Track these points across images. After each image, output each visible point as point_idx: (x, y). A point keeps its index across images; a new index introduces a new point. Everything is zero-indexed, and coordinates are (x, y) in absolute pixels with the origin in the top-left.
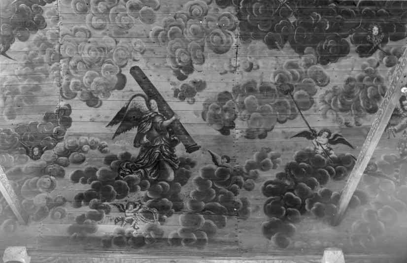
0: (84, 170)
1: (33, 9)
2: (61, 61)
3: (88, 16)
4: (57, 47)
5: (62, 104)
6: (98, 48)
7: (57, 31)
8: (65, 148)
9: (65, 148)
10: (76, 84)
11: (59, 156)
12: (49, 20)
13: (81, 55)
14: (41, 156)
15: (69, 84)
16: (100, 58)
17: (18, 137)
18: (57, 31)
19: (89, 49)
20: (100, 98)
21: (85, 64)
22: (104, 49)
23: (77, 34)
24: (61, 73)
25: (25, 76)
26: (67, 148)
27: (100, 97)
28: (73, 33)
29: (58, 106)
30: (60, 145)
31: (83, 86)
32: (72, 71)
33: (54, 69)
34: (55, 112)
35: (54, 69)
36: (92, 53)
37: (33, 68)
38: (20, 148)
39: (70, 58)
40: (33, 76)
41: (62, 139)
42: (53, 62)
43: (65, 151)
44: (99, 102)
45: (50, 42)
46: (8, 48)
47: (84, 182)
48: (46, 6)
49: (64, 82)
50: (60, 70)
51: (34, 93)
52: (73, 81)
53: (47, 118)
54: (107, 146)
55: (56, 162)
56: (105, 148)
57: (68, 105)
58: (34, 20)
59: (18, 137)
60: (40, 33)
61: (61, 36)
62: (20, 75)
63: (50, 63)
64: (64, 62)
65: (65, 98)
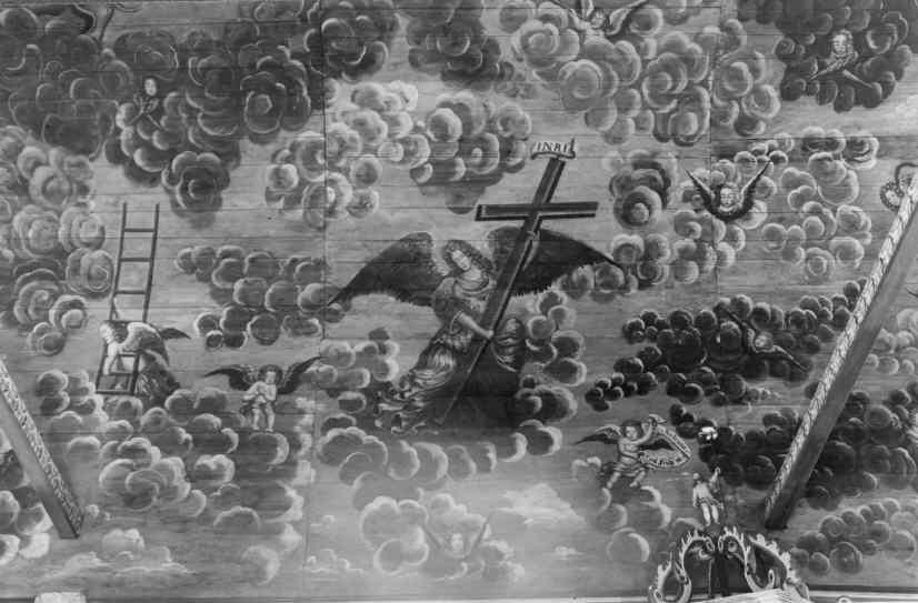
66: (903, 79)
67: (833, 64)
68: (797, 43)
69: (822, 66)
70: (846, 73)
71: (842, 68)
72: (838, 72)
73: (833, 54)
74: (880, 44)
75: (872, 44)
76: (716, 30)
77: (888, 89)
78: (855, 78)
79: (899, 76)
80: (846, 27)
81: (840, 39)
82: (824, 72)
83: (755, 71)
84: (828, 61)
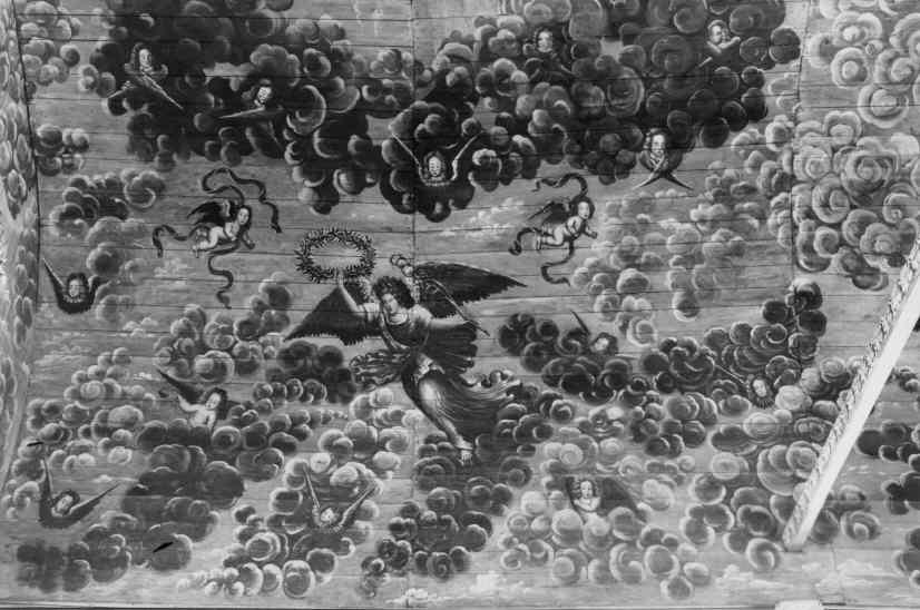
0: (881, 429)
1: (743, 76)
2: (795, 189)
3: (865, 91)
4: (785, 158)
5: (802, 281)
6: (878, 160)
7: (790, 124)
8: (821, 381)
9: (821, 381)
10: (825, 239)
11: (815, 399)
12: (774, 101)
13: (839, 175)
14: (773, 397)
15: (811, 238)
16: (882, 182)
17: (713, 356)
18: (790, 124)
19: (858, 161)
20: (883, 269)
21: (846, 193)
22: (891, 159)
23: (834, 130)
24: (795, 215)
25: (715, 223)
26: (825, 380)
27: (882, 264)
28: (824, 128)
29: (791, 288)
30: (809, 375)
31: (842, 243)
32: (818, 211)
33: (779, 207)
34: (786, 301)
35: (779, 207)
36: (866, 169)
37: (732, 207)
38: (722, 382)
39: (814, 183)
40: (732, 221)
41: (810, 362)
42: (776, 194)
43: (822, 390)
44: (881, 277)
45: (772, 148)
46: (675, 165)
47: (891, 455)
48: (774, 69)
49: (802, 235)
50: (791, 208)
51: (736, 261)
52: (820, 233)
53: (774, 312)
54: (914, 376)
55: (811, 411)
56: (912, 381)
57: (815, 286)
58: (743, 100)
59: (713, 356)
60: (751, 131)
61: (797, 135)
62: (703, 221)
63: (769, 194)
64: (801, 190)
65: (805, 271)
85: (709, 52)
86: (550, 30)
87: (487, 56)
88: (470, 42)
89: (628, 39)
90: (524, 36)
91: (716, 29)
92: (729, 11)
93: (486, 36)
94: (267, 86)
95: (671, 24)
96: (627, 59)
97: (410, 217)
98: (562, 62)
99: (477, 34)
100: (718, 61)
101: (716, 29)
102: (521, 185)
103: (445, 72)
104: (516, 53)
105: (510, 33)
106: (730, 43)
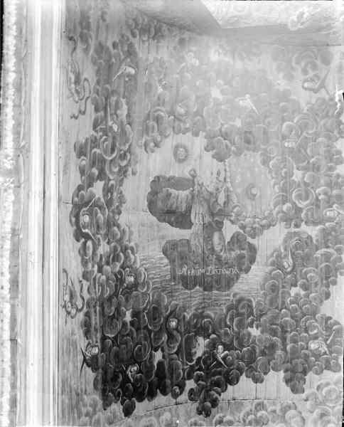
66: (331, 316)
67: (324, 348)
68: (315, 365)
69: (325, 353)
70: (328, 342)
71: (326, 344)
72: (329, 346)
73: (320, 349)
74: (315, 327)
75: (315, 331)
76: (308, 403)
77: (337, 323)
78: (331, 338)
79: (330, 318)
80: (307, 344)
81: (313, 346)
82: (328, 353)
83: (328, 384)
84: (323, 351)
85: (127, 368)
86: (135, 281)
87: (125, 250)
88: (129, 241)
89: (132, 323)
90: (132, 268)
91: (135, 368)
92: (142, 373)
93: (132, 249)
94: (118, 129)
95: (137, 344)
96: (124, 324)
97: (71, 202)
98: (123, 290)
99: (132, 244)
100: (124, 373)
101: (135, 368)
102: (80, 270)
103: (118, 227)
104: (125, 265)
105: (133, 260)
106: (130, 377)
